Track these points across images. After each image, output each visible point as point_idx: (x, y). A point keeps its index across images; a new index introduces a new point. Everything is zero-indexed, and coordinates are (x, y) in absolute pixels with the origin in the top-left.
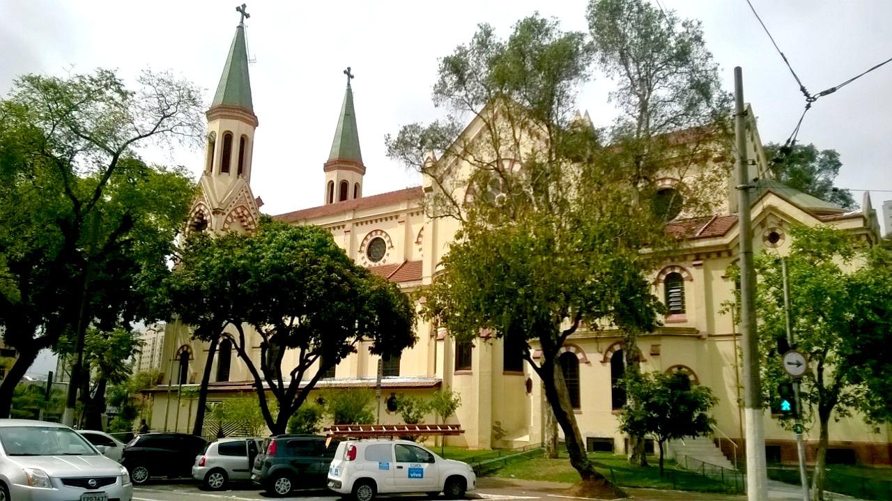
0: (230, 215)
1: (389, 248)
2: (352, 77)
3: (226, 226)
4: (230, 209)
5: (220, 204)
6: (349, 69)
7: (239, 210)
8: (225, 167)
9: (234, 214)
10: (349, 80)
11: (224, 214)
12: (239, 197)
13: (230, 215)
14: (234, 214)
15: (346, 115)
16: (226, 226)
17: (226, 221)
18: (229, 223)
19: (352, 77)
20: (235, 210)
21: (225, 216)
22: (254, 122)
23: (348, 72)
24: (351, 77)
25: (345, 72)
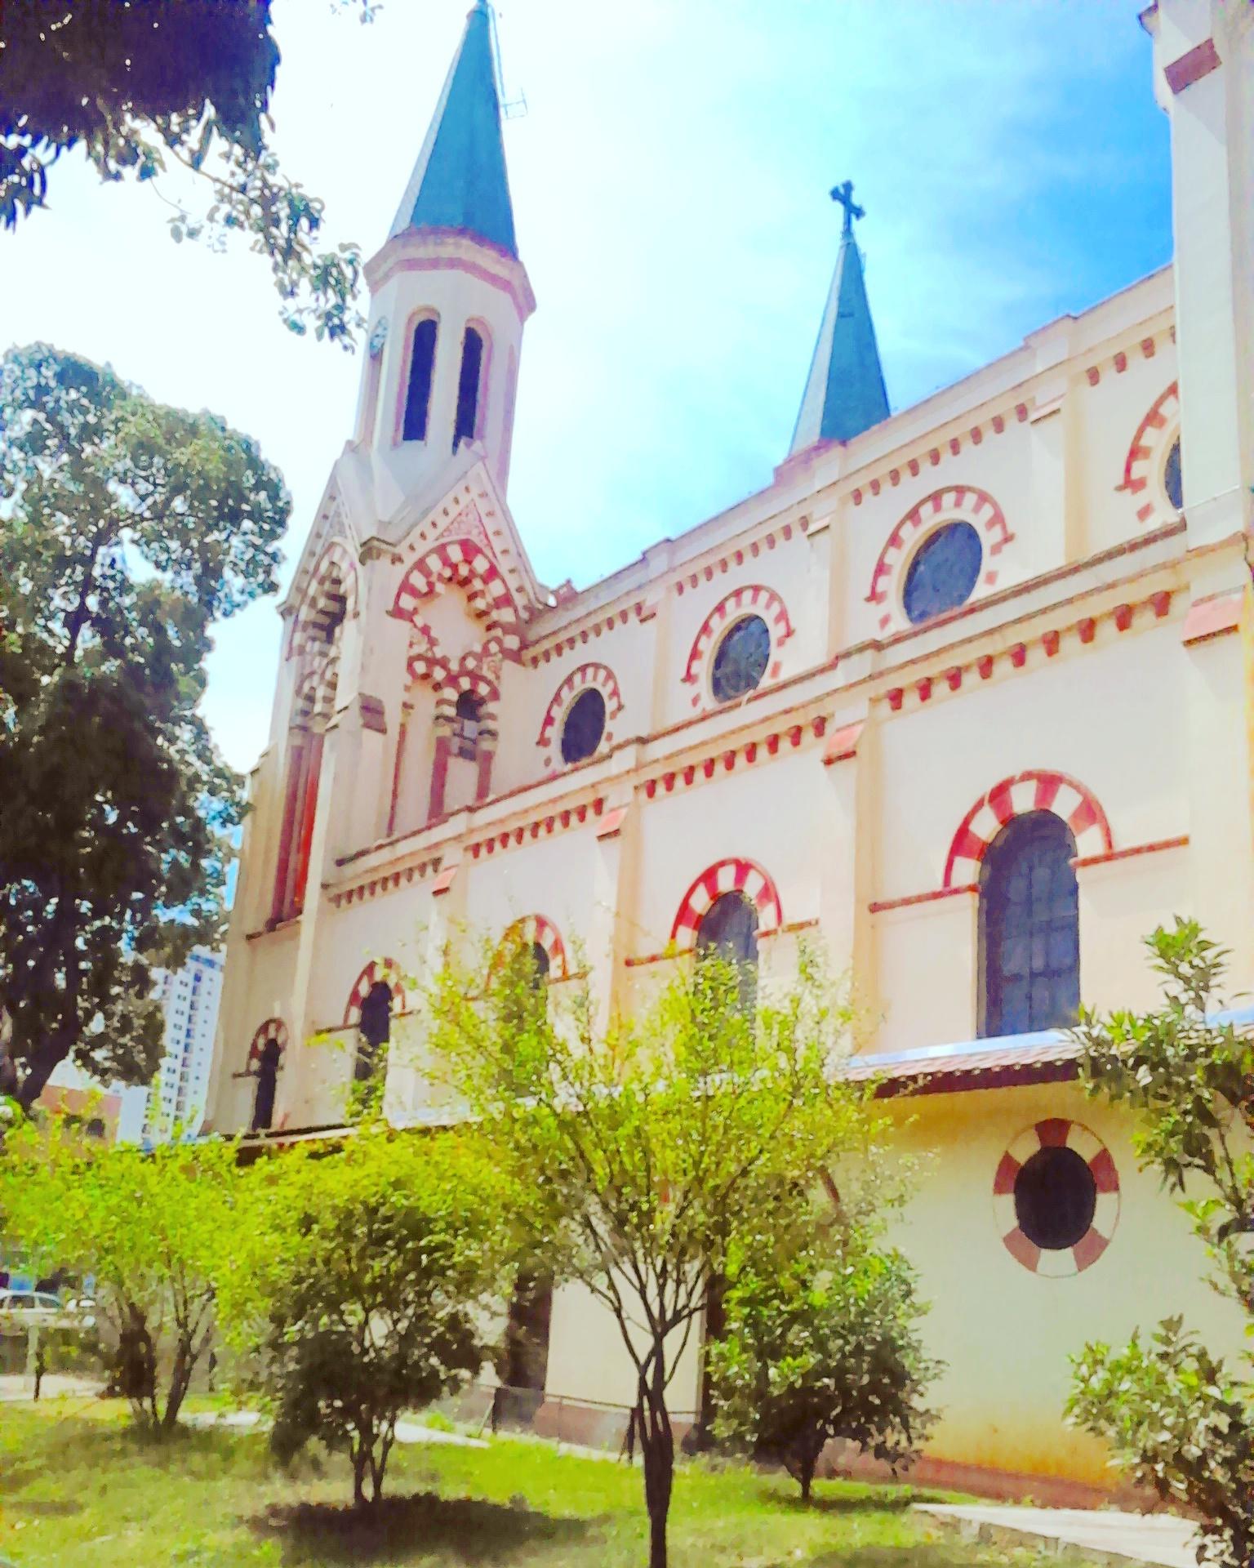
0: (420, 565)
1: (996, 549)
2: (859, 213)
3: (407, 602)
4: (422, 548)
5: (383, 525)
6: (848, 187)
7: (455, 554)
8: (414, 425)
9: (434, 563)
10: (848, 222)
11: (396, 559)
12: (454, 511)
13: (420, 565)
14: (434, 563)
15: (841, 315)
16: (407, 602)
17: (406, 587)
18: (414, 592)
19: (859, 213)
20: (441, 550)
21: (400, 571)
22: (525, 304)
23: (842, 194)
24: (854, 211)
25: (835, 194)
